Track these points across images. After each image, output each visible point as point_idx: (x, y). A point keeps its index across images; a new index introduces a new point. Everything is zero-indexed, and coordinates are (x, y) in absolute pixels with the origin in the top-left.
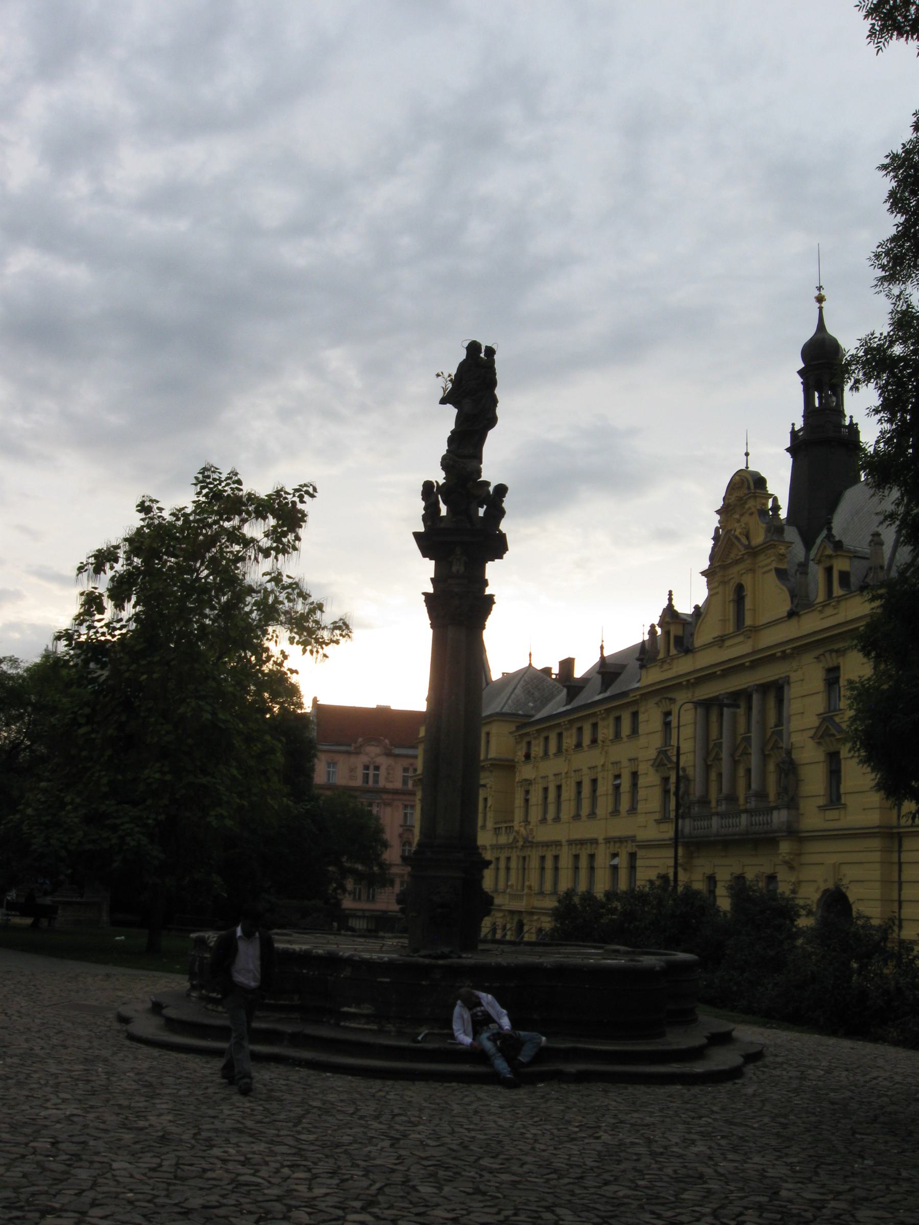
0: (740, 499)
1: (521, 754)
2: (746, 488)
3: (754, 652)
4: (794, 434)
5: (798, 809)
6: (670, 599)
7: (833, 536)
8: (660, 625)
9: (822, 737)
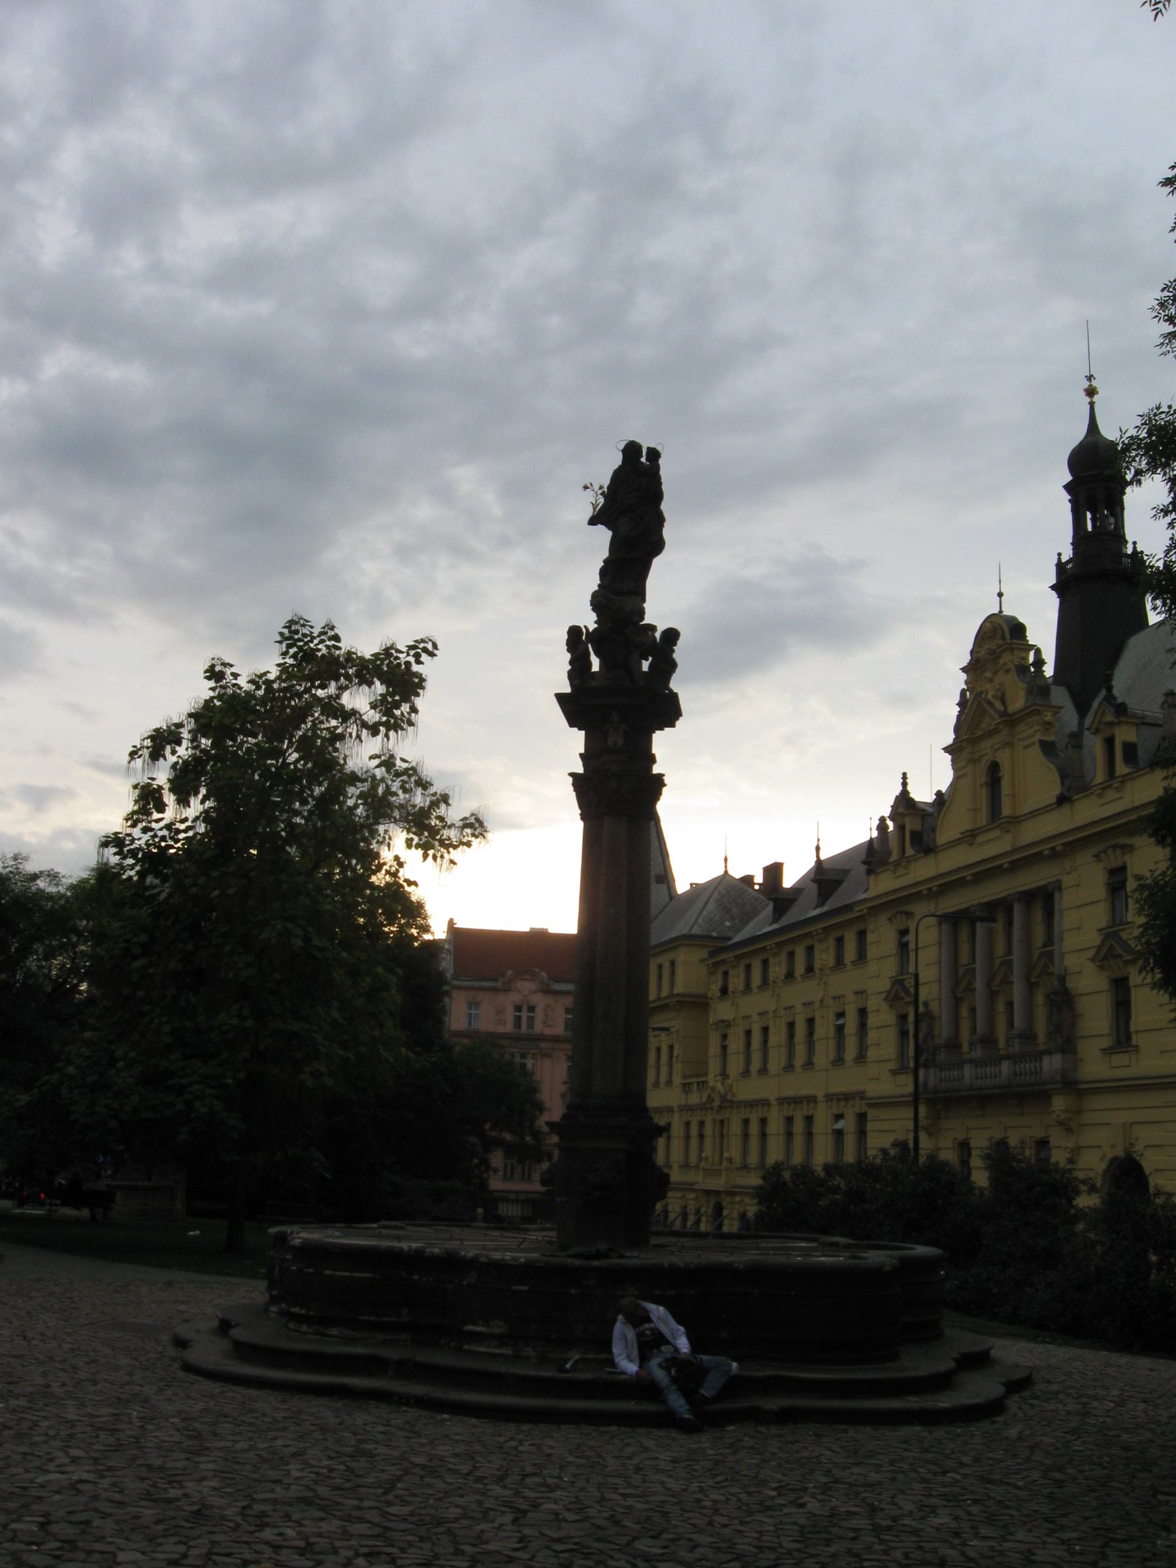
0: (992, 652)
1: (715, 989)
2: (1000, 638)
3: (1015, 850)
4: (1060, 566)
5: (1075, 1053)
6: (904, 784)
7: (1114, 698)
8: (892, 818)
9: (1104, 958)
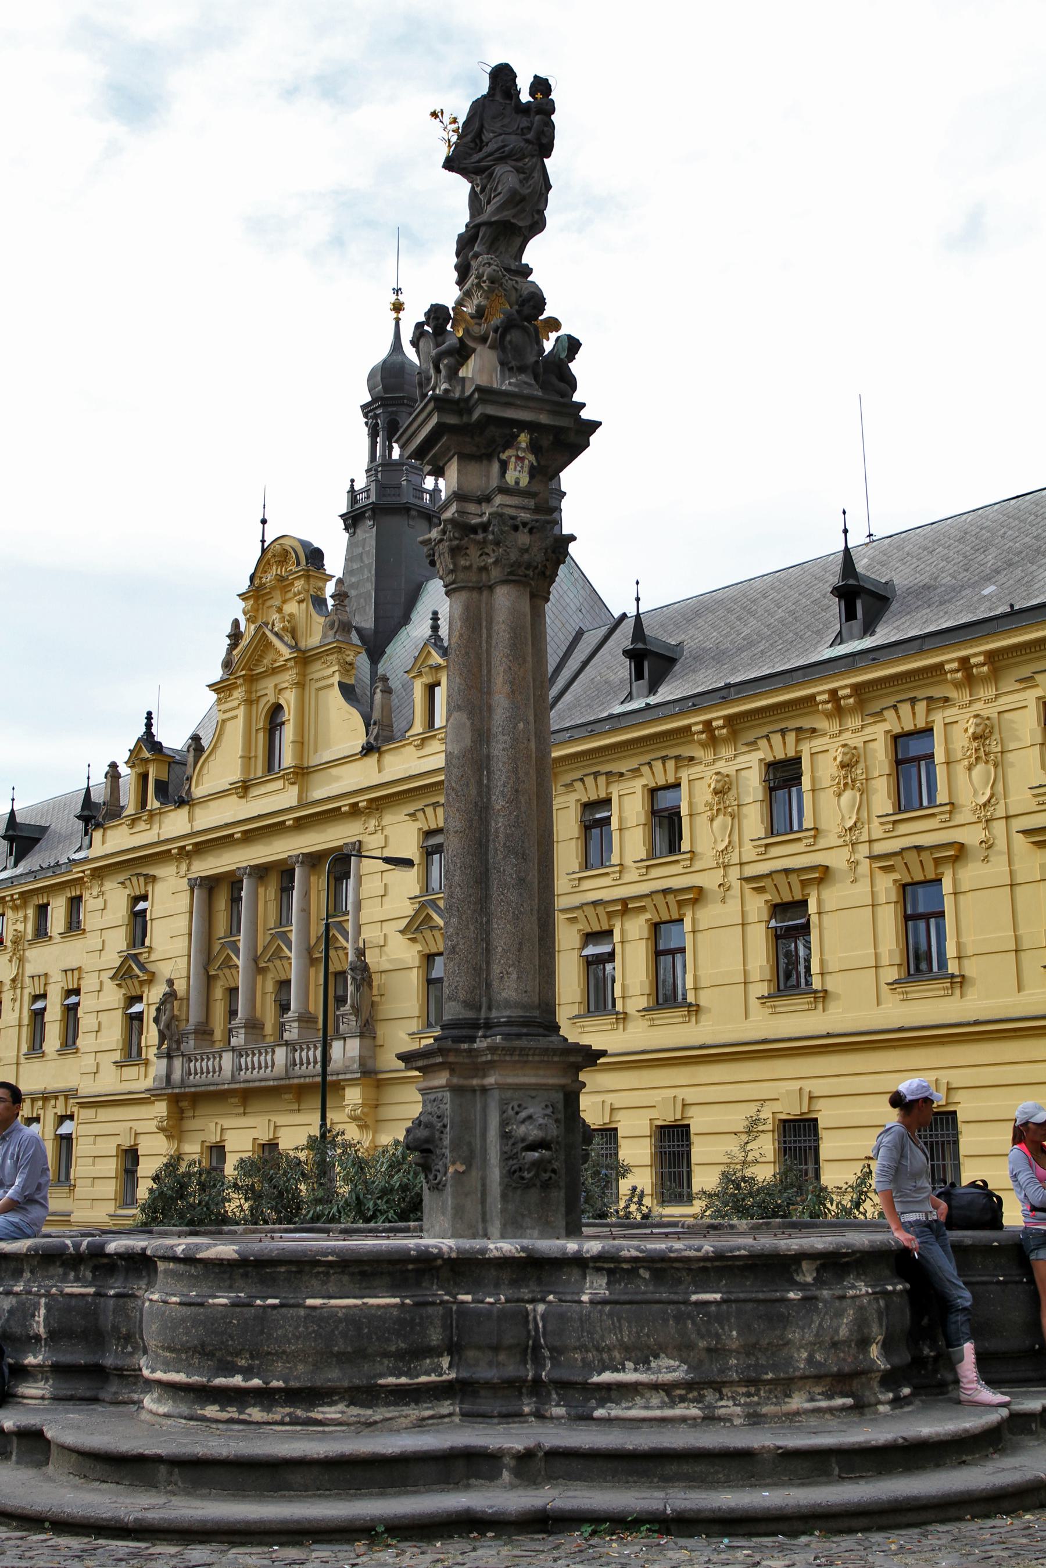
6: (149, 725)
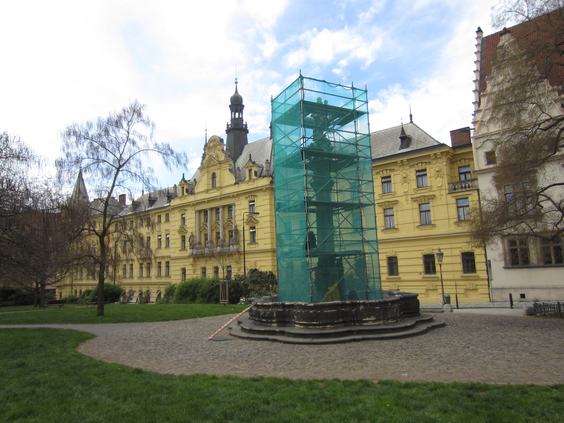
3: (221, 195)
6: (183, 176)
